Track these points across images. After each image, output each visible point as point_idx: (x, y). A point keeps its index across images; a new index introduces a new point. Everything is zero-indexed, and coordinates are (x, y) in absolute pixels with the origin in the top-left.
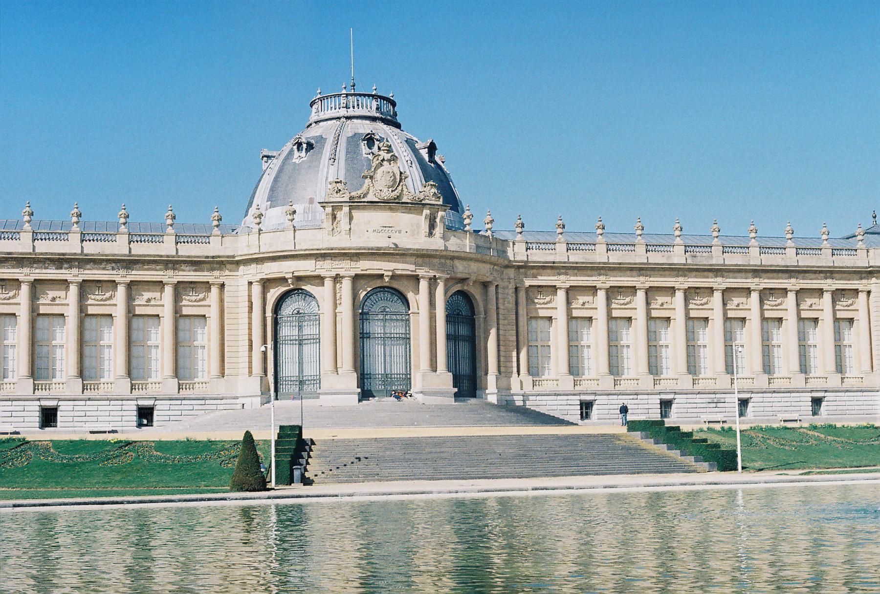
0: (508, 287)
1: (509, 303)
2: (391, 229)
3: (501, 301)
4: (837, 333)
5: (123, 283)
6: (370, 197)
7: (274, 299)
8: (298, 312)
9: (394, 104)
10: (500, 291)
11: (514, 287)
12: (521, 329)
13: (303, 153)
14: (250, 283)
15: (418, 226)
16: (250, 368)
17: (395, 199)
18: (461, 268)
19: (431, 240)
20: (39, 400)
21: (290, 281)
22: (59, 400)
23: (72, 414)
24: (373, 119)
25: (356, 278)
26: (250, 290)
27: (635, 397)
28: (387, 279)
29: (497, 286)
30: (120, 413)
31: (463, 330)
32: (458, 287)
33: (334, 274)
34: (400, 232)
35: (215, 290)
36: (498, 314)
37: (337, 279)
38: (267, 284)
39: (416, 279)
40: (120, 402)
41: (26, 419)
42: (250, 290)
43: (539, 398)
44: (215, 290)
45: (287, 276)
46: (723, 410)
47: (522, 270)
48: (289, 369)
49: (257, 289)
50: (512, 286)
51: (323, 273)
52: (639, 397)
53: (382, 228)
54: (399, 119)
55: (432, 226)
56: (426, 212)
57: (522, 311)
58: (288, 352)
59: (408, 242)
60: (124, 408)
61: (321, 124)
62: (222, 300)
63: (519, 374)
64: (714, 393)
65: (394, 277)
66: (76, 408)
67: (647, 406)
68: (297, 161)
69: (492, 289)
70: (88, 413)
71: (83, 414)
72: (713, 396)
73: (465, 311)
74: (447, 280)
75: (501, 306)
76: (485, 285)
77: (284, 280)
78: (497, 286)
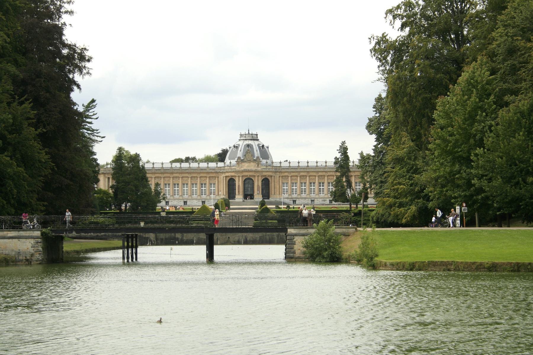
9: (257, 135)
18: (264, 174)
24: (251, 140)
25: (243, 176)
29: (274, 176)
35: (217, 178)
36: (274, 182)
37: (239, 176)
38: (226, 177)
39: (255, 176)
44: (217, 178)
49: (224, 178)
50: (278, 176)
51: (236, 175)
54: (259, 138)
55: (258, 165)
57: (281, 181)
62: (218, 180)
65: (250, 176)
69: (273, 177)
76: (271, 176)
77: (229, 176)
78: (274, 176)
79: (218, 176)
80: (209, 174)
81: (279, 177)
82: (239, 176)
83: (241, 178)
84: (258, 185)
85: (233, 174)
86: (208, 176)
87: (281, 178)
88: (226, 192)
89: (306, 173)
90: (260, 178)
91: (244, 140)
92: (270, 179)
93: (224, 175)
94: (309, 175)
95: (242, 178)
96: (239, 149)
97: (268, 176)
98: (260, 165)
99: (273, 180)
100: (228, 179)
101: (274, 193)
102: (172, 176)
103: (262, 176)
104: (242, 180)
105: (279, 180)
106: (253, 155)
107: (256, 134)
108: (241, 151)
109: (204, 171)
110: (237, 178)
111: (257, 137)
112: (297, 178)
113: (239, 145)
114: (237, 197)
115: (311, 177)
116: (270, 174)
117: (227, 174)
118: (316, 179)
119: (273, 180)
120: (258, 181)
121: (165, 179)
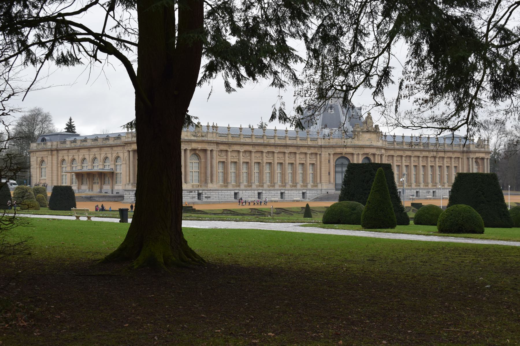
22: (285, 190)
33: (357, 153)
35: (318, 156)
59: (375, 144)
79: (320, 153)
86: (309, 152)
93: (332, 151)
117: (339, 150)
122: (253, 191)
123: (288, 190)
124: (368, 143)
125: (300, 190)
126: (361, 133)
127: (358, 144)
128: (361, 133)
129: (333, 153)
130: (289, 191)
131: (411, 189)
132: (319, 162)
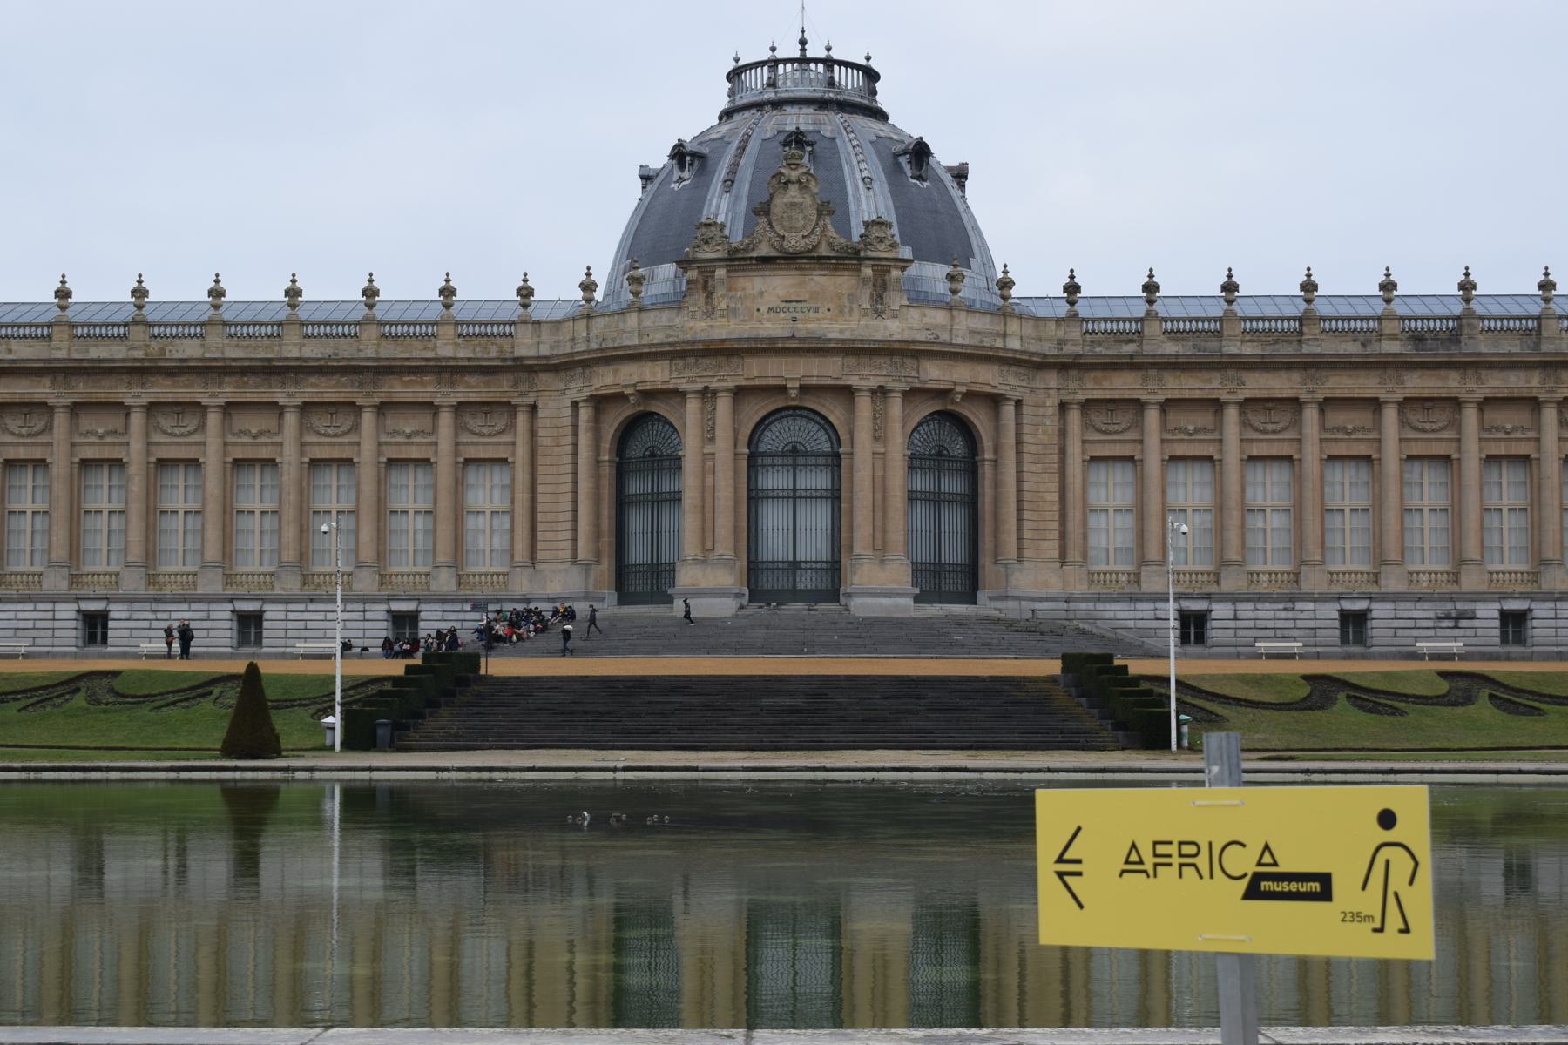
0: (1044, 402)
1: (1044, 433)
2: (800, 305)
3: (1026, 429)
4: (383, 497)
5: (369, 406)
6: (764, 250)
7: (612, 431)
8: (940, 452)
9: (871, 76)
10: (1025, 410)
11: (1056, 403)
12: (1070, 480)
13: (686, 174)
14: (575, 404)
15: (852, 298)
16: (574, 549)
17: (809, 251)
18: (934, 373)
19: (877, 323)
20: (231, 601)
21: (632, 400)
22: (264, 601)
23: (282, 625)
24: (822, 104)
25: (740, 393)
26: (576, 415)
27: (1289, 605)
28: (793, 393)
29: (1018, 403)
30: (360, 625)
31: (953, 484)
32: (936, 406)
33: (699, 386)
34: (816, 310)
35: (522, 419)
36: (1019, 453)
37: (707, 394)
38: (600, 402)
39: (846, 393)
40: (360, 607)
41: (213, 633)
42: (576, 415)
43: (1100, 606)
44: (522, 419)
45: (628, 391)
46: (1470, 632)
47: (1073, 373)
48: (639, 553)
49: (585, 414)
50: (1052, 401)
51: (683, 385)
52: (1299, 605)
53: (784, 304)
54: (884, 100)
55: (878, 298)
56: (868, 272)
58: (638, 521)
60: (368, 616)
61: (737, 117)
62: (533, 434)
63: (1063, 563)
64: (1452, 599)
65: (805, 389)
66: (291, 616)
67: (1311, 624)
68: (674, 186)
69: (1009, 410)
70: (310, 625)
71: (301, 625)
72: (1449, 606)
73: (958, 448)
74: (905, 394)
75: (1026, 438)
76: (994, 401)
77: (620, 398)
78: (1018, 403)
79: (530, 399)
80: (453, 384)
81: (1063, 407)
82: (707, 394)
83: (724, 405)
84: (881, 486)
85: (657, 374)
87: (1074, 417)
88: (597, 535)
89: (1296, 376)
90: (896, 407)
91: (759, 106)
92: (979, 418)
93: (580, 387)
94: (1320, 397)
95: (736, 411)
96: (722, 172)
97: (970, 396)
98: (895, 300)
99: (1009, 439)
100: (614, 420)
101: (1020, 549)
102: (135, 395)
103: (912, 394)
104: (736, 432)
105: (1063, 433)
106: (832, 208)
107: (864, 62)
108: (729, 183)
109: (417, 352)
110: (693, 405)
111: (874, 93)
112: (1219, 426)
113: (723, 141)
114: (687, 577)
115: (1338, 418)
116: (989, 377)
117: (606, 379)
118: (1378, 426)
119: (1009, 439)
120: (879, 436)
121: (87, 422)
122: (49, 606)
123: (287, 602)
124: (773, 328)
125: (375, 601)
126: (720, 273)
127: (704, 336)
128: (720, 273)
129: (586, 393)
130: (291, 607)
131: (1293, 599)
132: (521, 453)
